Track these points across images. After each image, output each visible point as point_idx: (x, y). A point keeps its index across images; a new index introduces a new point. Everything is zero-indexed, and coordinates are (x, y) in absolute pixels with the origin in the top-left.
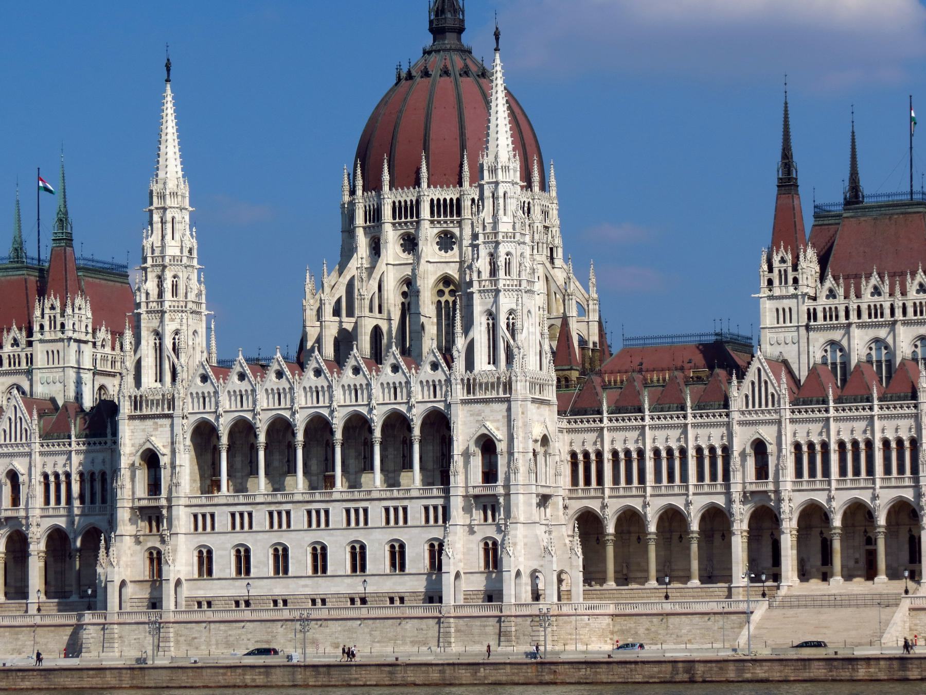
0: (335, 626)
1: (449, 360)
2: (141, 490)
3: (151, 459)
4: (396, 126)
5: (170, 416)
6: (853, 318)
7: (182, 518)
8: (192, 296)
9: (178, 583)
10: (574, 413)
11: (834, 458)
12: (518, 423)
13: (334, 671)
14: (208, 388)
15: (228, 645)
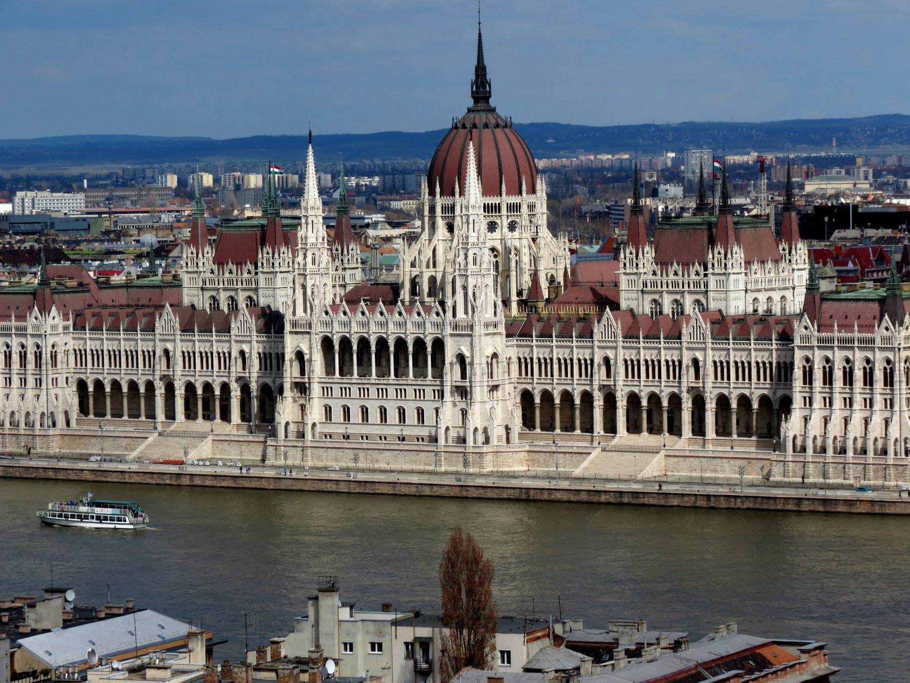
0: (388, 453)
1: (444, 312)
2: (296, 372)
3: (300, 355)
4: (446, 158)
5: (309, 333)
6: (665, 288)
7: (316, 390)
8: (323, 265)
9: (314, 425)
10: (520, 336)
11: (643, 369)
12: (477, 348)
13: (368, 485)
14: (327, 318)
15: (337, 460)
